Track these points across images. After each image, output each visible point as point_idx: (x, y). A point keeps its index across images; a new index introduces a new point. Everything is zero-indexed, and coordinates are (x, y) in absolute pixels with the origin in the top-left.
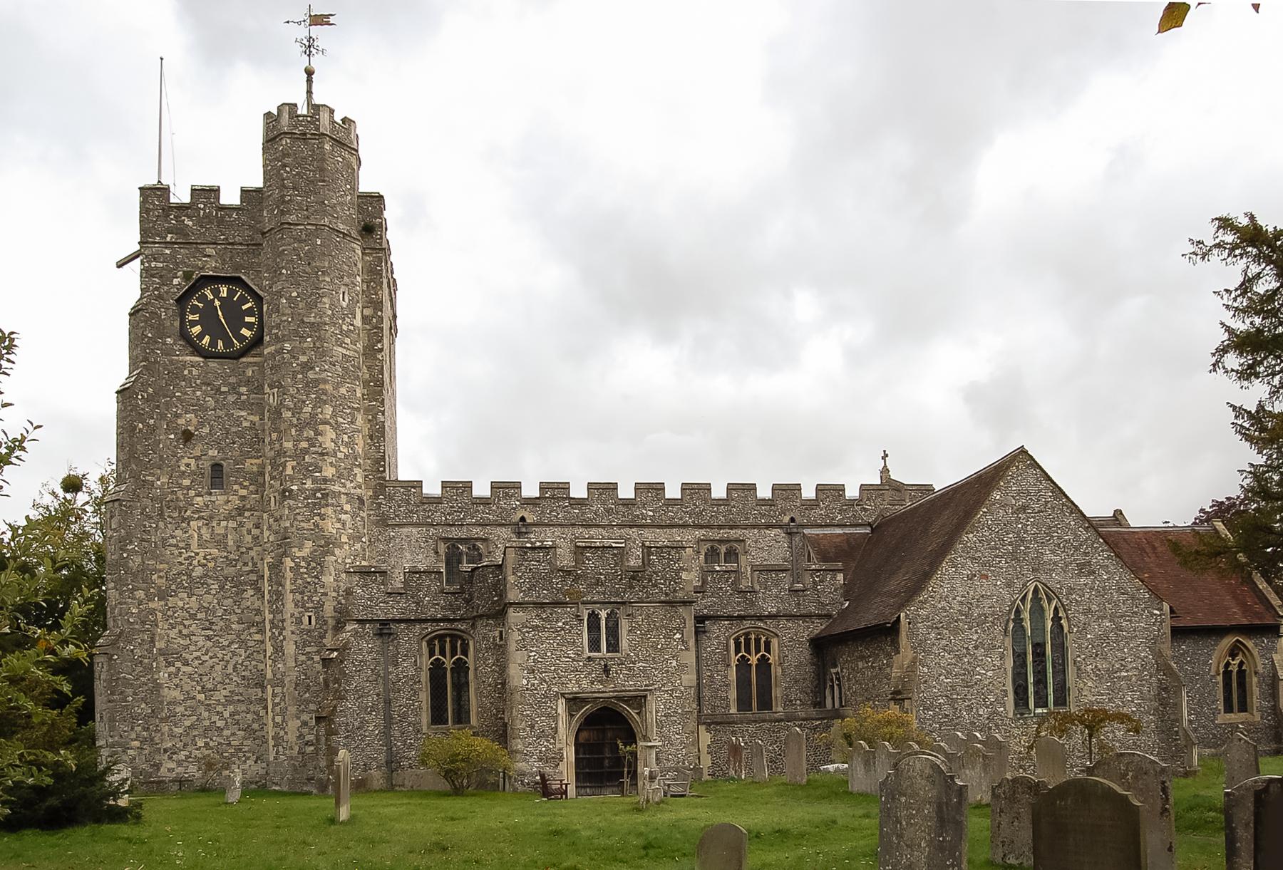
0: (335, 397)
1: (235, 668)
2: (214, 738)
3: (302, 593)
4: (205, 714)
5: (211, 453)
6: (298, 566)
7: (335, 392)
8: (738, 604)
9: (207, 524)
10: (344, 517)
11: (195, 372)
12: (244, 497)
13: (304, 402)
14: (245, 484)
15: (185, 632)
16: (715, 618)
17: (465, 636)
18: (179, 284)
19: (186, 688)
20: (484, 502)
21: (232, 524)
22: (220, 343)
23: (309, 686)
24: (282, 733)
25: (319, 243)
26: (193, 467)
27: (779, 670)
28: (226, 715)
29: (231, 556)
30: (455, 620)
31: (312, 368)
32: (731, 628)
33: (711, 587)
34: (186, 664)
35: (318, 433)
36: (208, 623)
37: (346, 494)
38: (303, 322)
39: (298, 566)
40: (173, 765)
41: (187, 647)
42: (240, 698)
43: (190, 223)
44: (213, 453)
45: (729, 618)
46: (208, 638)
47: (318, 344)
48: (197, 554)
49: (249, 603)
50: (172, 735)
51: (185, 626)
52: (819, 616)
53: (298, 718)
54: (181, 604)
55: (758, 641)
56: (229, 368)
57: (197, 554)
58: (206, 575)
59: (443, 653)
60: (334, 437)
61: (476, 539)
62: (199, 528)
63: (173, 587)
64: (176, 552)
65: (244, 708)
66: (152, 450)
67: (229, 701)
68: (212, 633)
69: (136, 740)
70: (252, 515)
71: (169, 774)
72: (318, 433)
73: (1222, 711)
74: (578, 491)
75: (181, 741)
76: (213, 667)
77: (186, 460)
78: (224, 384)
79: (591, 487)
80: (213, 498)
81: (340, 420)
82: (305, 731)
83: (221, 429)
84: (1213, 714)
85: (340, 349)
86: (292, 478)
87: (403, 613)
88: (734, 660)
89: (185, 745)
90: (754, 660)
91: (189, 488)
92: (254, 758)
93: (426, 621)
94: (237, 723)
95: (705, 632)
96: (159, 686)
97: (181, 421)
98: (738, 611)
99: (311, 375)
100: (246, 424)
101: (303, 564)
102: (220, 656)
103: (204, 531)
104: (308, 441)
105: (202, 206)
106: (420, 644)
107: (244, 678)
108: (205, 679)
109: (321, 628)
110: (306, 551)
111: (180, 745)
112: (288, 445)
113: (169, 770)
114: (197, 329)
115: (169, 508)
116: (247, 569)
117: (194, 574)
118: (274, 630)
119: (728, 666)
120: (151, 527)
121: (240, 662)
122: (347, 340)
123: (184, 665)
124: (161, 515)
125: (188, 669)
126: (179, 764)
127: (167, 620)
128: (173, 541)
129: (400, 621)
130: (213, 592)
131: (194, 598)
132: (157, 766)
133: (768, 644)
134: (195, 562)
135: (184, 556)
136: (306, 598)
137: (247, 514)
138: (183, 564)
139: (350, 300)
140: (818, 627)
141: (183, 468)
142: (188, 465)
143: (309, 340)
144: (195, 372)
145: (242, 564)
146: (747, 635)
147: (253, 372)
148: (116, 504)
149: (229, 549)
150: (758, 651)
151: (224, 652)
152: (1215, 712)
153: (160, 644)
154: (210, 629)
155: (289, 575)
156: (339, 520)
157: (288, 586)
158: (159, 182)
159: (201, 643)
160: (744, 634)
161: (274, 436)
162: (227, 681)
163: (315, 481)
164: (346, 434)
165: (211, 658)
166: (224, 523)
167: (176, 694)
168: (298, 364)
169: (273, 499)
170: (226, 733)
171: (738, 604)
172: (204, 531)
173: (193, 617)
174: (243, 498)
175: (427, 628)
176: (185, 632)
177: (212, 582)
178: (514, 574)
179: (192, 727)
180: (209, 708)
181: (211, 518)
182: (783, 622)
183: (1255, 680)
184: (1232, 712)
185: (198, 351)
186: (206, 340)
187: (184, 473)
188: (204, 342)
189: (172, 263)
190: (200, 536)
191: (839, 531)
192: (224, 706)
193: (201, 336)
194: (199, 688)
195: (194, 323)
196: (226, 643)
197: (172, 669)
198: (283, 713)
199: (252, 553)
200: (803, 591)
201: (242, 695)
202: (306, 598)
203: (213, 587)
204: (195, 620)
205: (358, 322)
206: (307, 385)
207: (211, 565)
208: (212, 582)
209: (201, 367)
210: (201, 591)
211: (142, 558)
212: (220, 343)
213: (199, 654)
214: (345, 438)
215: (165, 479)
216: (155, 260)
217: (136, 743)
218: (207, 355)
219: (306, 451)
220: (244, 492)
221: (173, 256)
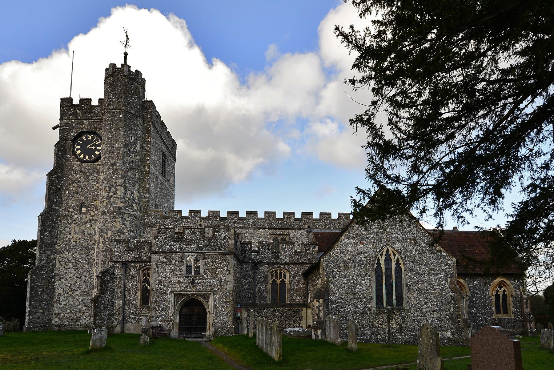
0: (125, 176)
1: (84, 281)
2: (74, 309)
3: (106, 252)
4: (72, 300)
5: (81, 198)
7: (125, 175)
8: (272, 258)
9: (78, 226)
10: (126, 222)
11: (77, 168)
13: (112, 178)
14: (93, 210)
15: (66, 267)
16: (262, 263)
18: (74, 135)
20: (186, 218)
21: (87, 226)
22: (87, 157)
25: (121, 117)
27: (289, 286)
28: (80, 300)
31: (116, 165)
32: (269, 268)
33: (261, 250)
34: (66, 280)
35: (117, 190)
37: (128, 214)
38: (113, 147)
39: (105, 241)
41: (66, 273)
42: (86, 293)
43: (79, 112)
44: (82, 198)
45: (268, 263)
46: (75, 270)
47: (118, 156)
48: (73, 237)
50: (58, 307)
51: (66, 265)
52: (307, 264)
55: (281, 273)
56: (90, 166)
57: (73, 237)
58: (76, 245)
60: (124, 192)
62: (75, 227)
63: (63, 250)
65: (87, 297)
66: (58, 197)
67: (81, 295)
68: (77, 268)
69: (41, 309)
70: (95, 222)
71: (55, 323)
72: (117, 190)
73: (495, 312)
74: (223, 214)
75: (61, 310)
76: (76, 281)
77: (72, 201)
78: (88, 172)
79: (229, 212)
81: (127, 185)
83: (86, 190)
84: (490, 313)
85: (129, 158)
86: (106, 207)
87: (133, 259)
88: (270, 282)
90: (278, 281)
91: (72, 212)
94: (84, 303)
95: (258, 269)
97: (71, 186)
98: (273, 261)
99: (115, 167)
100: (95, 188)
101: (107, 240)
102: (79, 277)
103: (76, 228)
104: (113, 192)
105: (84, 105)
107: (87, 285)
108: (72, 286)
110: (109, 236)
114: (79, 152)
116: (92, 243)
119: (267, 283)
120: (56, 226)
122: (132, 155)
125: (66, 282)
127: (60, 263)
129: (131, 262)
133: (285, 275)
135: (68, 238)
136: (108, 254)
138: (67, 241)
139: (134, 140)
141: (70, 204)
142: (72, 203)
143: (115, 154)
144: (77, 168)
145: (90, 241)
146: (276, 271)
147: (99, 168)
150: (280, 278)
152: (492, 313)
153: (57, 272)
156: (124, 224)
158: (70, 97)
159: (72, 272)
160: (275, 270)
162: (81, 287)
163: (115, 208)
164: (130, 190)
165: (75, 277)
167: (61, 292)
168: (110, 163)
170: (79, 307)
171: (272, 258)
172: (76, 228)
173: (70, 261)
174: (92, 216)
175: (142, 265)
176: (66, 267)
177: (78, 248)
179: (66, 304)
180: (73, 298)
182: (292, 266)
183: (511, 299)
184: (500, 313)
185: (80, 160)
186: (82, 156)
188: (81, 156)
189: (71, 127)
190: (75, 230)
191: (328, 231)
192: (79, 296)
193: (80, 154)
194: (70, 289)
195: (78, 149)
197: (60, 282)
199: (94, 237)
200: (301, 253)
202: (108, 254)
203: (78, 250)
204: (70, 262)
205: (138, 148)
206: (114, 171)
207: (79, 241)
208: (78, 248)
209: (80, 166)
211: (50, 238)
212: (87, 157)
213: (71, 276)
214: (129, 192)
216: (65, 126)
217: (41, 311)
218: (82, 161)
219: (112, 197)
220: (93, 214)
221: (72, 124)
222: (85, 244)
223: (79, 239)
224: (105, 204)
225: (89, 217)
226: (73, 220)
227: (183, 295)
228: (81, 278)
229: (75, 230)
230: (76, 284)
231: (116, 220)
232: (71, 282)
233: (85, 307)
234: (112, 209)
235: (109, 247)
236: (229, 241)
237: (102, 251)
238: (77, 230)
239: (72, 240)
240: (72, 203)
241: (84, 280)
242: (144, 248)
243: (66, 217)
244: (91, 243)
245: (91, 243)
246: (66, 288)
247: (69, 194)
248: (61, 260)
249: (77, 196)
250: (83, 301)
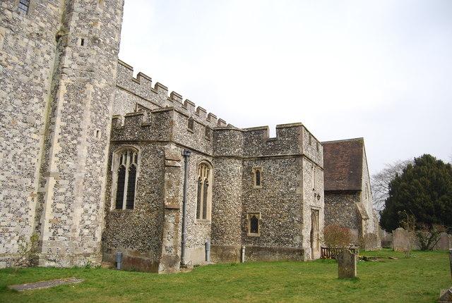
3: (96, 113)
6: (96, 93)
9: (13, 35)
12: (42, 28)
14: (44, 19)
21: (32, 44)
23: (92, 182)
24: (64, 218)
29: (27, 67)
39: (96, 93)
42: (14, 184)
49: (33, 108)
53: (83, 207)
62: (6, 35)
82: (86, 217)
92: (17, 238)
101: (99, 93)
109: (103, 141)
118: (66, 135)
121: (19, 153)
130: (8, 90)
136: (98, 117)
137: (43, 41)
149: (26, 61)
151: (8, 143)
155: (90, 97)
157: (89, 105)
162: (6, 168)
163: (111, 41)
174: (41, 29)
181: (17, 33)
196: (11, 135)
198: (69, 202)
199: (42, 71)
201: (16, 182)
220: (43, 25)
222: (24, 78)
223: (14, 64)
224: (99, 27)
228: (9, 148)
233: (11, 215)
234: (108, 41)
235: (101, 105)
237: (90, 110)
241: (13, 153)
244: (35, 80)
245: (35, 80)
250: (9, 201)
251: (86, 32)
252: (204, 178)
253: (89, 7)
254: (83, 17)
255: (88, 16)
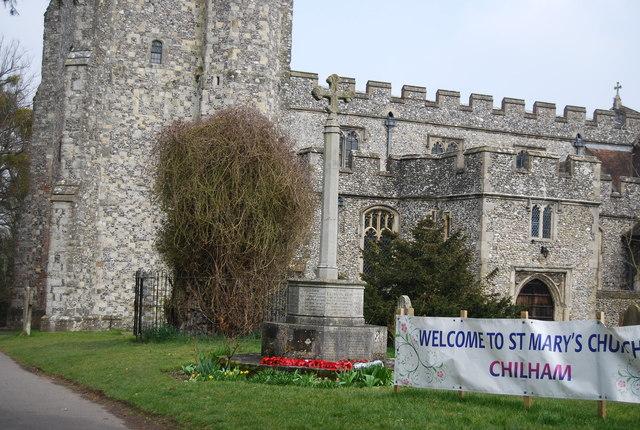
4: (135, 261)
10: (271, 100)
15: (123, 186)
17: (393, 212)
19: (121, 236)
21: (168, 95)
26: (138, 42)
30: (387, 198)
34: (122, 215)
35: (259, 28)
36: (142, 180)
40: (103, 305)
41: (122, 200)
44: (155, 30)
50: (105, 278)
54: (121, 161)
57: (138, 118)
59: (375, 225)
61: (357, 128)
62: (141, 96)
64: (120, 115)
72: (259, 28)
80: (153, 71)
89: (116, 287)
93: (365, 197)
96: (98, 233)
100: (184, 9)
103: (145, 98)
106: (360, 215)
108: (137, 229)
111: (111, 287)
112: (234, 34)
113: (100, 309)
115: (117, 74)
117: (133, 136)
123: (120, 215)
124: (110, 81)
125: (123, 220)
126: (110, 304)
128: (118, 105)
131: (133, 157)
132: (92, 305)
134: (136, 126)
137: (181, 87)
140: (628, 226)
142: (134, 40)
148: (81, 69)
153: (102, 196)
154: (144, 186)
161: (219, 25)
163: (254, 67)
165: (143, 211)
166: (162, 94)
167: (111, 241)
169: (215, 79)
172: (145, 98)
173: (131, 174)
174: (178, 73)
178: (489, 172)
180: (138, 256)
187: (130, 46)
190: (141, 103)
197: (110, 219)
207: (149, 129)
210: (139, 152)
215: (114, 49)
219: (248, 42)
220: (178, 68)
223: (152, 124)
225: (174, 77)
226: (136, 78)
227: (526, 273)
229: (141, 103)
230: (144, 226)
231: (260, 94)
232: (134, 222)
234: (249, 69)
236: (594, 183)
238: (147, 103)
239: (136, 126)
240: (134, 40)
242: (370, 169)
243: (122, 72)
246: (122, 234)
247: (127, 17)
248: (111, 169)
249: (144, 24)
251: (220, 67)
252: (379, 233)
253: (223, 33)
254: (217, 49)
255: (223, 46)
